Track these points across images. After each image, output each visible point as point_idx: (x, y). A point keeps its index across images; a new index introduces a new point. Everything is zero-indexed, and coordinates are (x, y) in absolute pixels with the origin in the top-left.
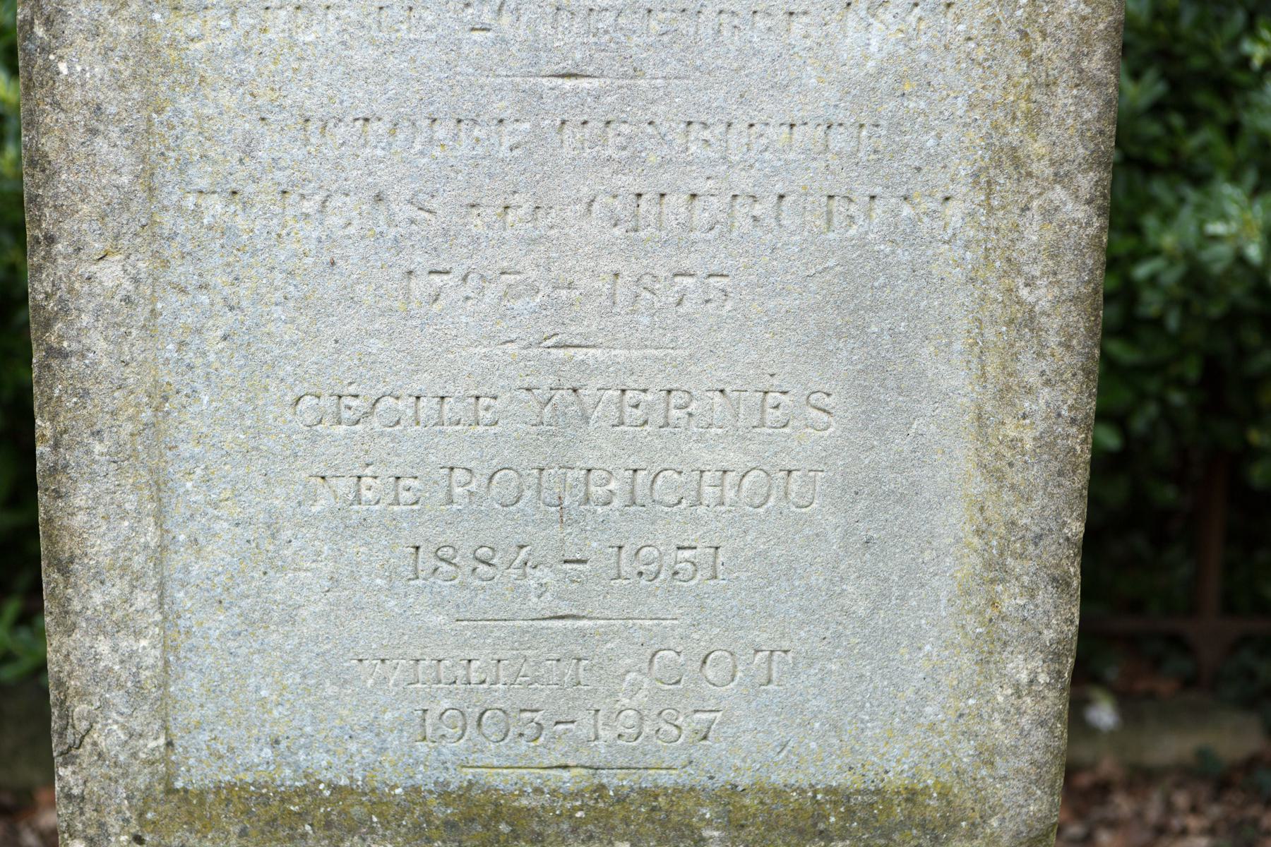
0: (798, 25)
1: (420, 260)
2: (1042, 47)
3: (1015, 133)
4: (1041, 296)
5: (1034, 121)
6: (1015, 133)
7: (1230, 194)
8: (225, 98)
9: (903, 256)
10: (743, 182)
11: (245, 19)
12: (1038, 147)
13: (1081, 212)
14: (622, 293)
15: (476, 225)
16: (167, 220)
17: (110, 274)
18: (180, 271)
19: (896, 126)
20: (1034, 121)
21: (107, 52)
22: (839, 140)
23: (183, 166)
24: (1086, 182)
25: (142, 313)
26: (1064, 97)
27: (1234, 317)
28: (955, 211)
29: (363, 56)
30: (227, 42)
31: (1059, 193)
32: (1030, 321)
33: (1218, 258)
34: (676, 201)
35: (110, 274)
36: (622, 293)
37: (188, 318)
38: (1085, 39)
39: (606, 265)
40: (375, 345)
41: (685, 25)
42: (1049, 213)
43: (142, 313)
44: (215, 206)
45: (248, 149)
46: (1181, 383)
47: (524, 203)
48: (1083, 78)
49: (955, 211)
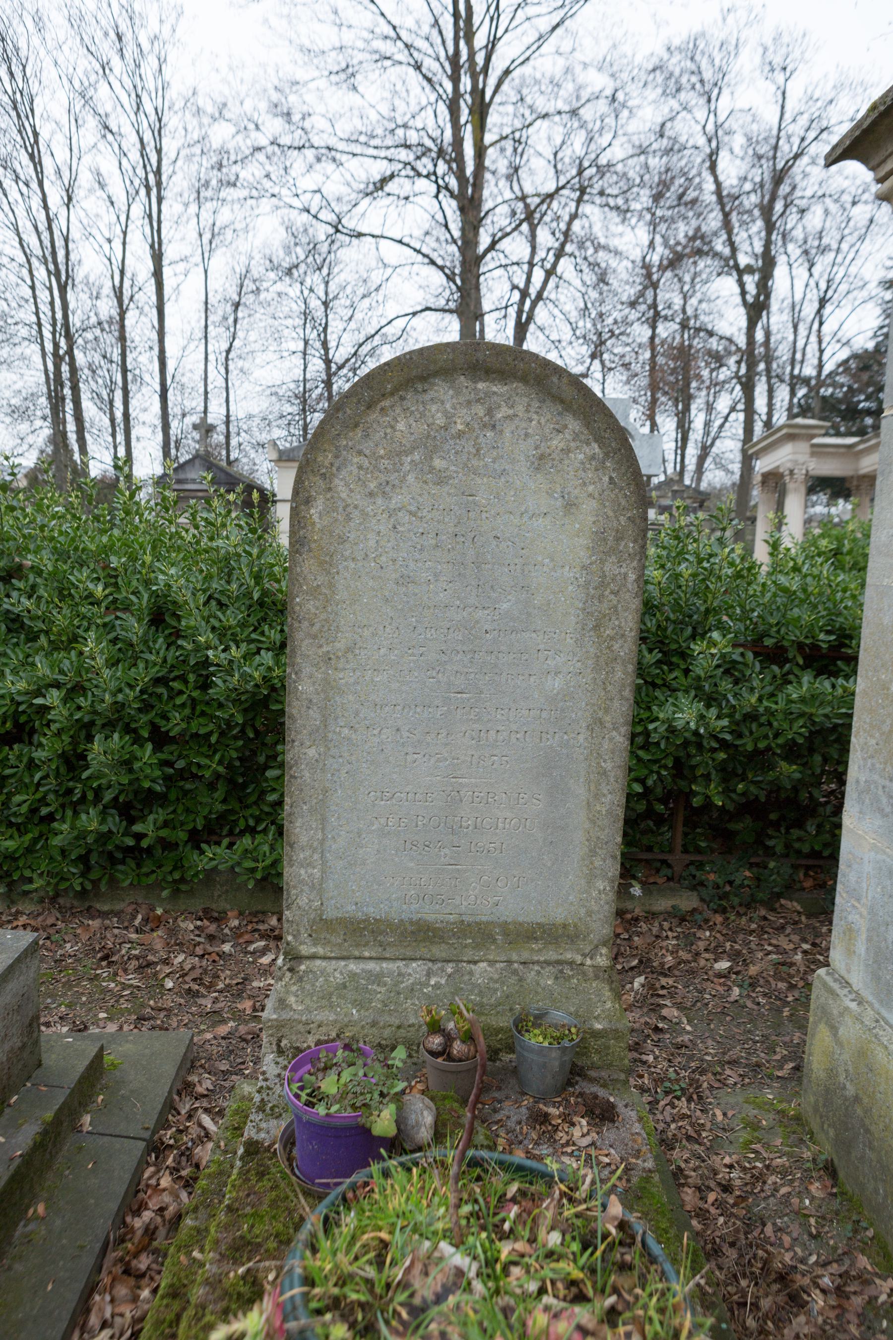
0: (532, 679)
1: (410, 750)
2: (609, 688)
3: (600, 714)
4: (608, 765)
5: (607, 710)
6: (600, 714)
7: (684, 701)
8: (351, 698)
9: (564, 751)
10: (514, 727)
11: (358, 673)
12: (608, 718)
13: (621, 739)
14: (475, 761)
15: (429, 739)
16: (330, 735)
17: (312, 752)
18: (333, 751)
19: (563, 710)
20: (607, 710)
21: (314, 683)
22: (544, 714)
23: (336, 719)
24: (624, 730)
25: (321, 765)
26: (616, 704)
27: (686, 743)
28: (581, 738)
29: (395, 686)
30: (352, 680)
31: (614, 733)
32: (605, 773)
33: (679, 724)
34: (492, 733)
35: (312, 752)
36: (475, 761)
37: (335, 766)
38: (623, 685)
39: (470, 752)
40: (395, 776)
41: (496, 678)
42: (611, 739)
43: (321, 765)
44: (346, 731)
45: (357, 714)
46: (665, 767)
47: (444, 732)
48: (622, 698)
49: (581, 738)
